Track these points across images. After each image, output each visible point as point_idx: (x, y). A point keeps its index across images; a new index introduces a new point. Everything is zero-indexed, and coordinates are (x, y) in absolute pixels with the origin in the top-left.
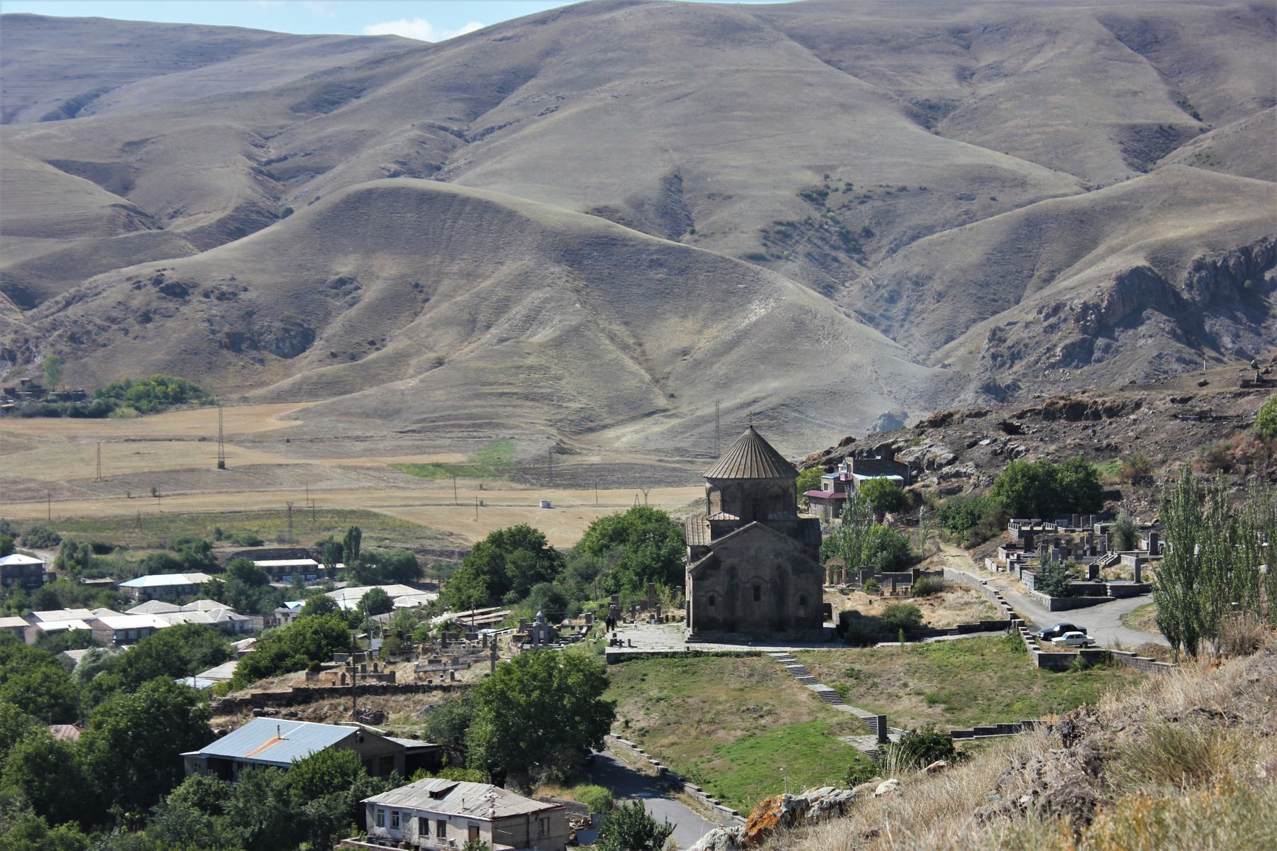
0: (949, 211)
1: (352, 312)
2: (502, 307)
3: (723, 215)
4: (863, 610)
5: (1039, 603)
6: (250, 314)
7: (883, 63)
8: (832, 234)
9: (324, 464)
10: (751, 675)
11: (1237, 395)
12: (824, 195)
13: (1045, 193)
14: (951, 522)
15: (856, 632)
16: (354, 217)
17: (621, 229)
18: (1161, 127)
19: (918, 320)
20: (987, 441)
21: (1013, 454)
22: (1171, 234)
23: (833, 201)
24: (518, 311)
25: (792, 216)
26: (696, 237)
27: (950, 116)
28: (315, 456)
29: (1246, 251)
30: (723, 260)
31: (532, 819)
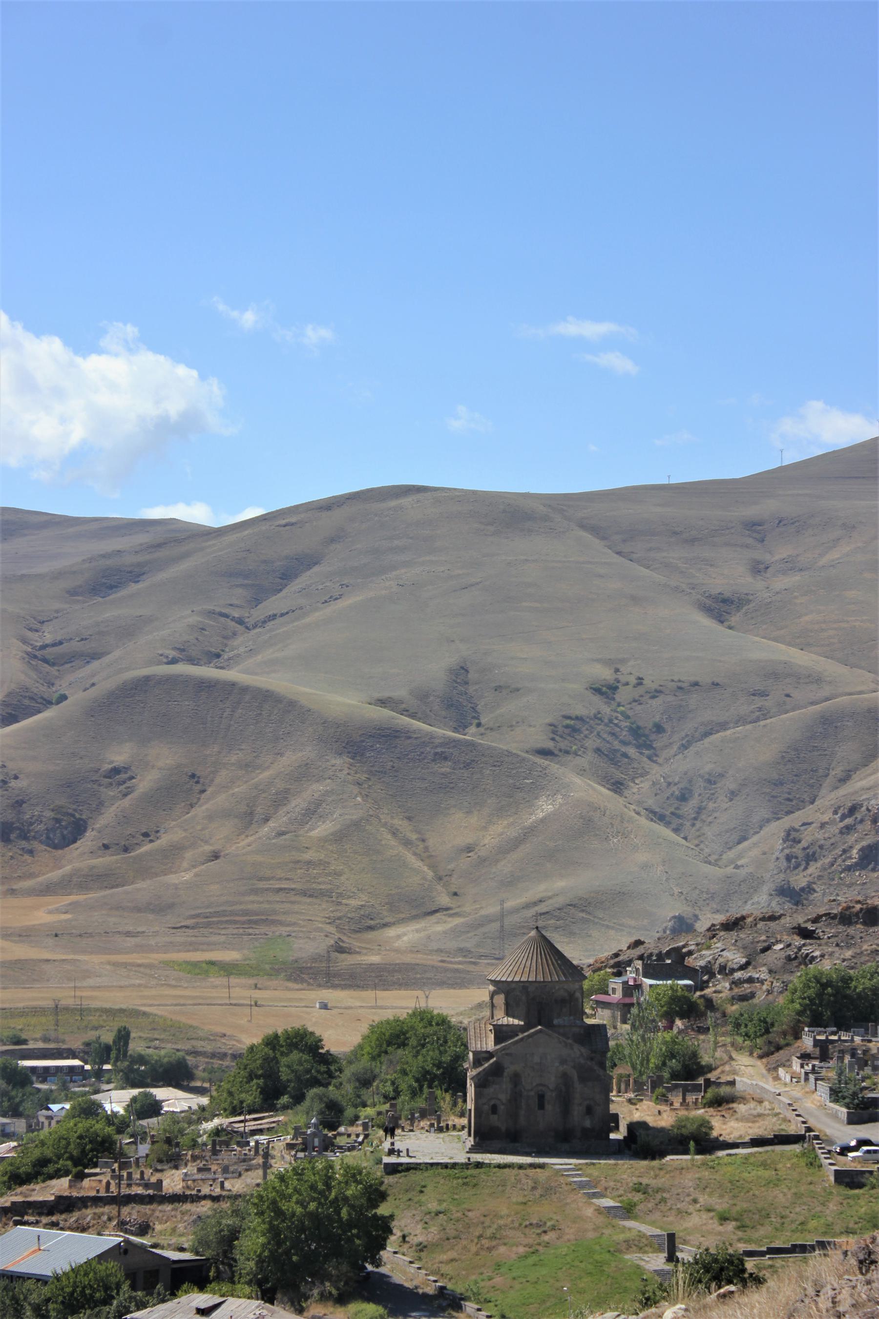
1: (126, 802)
2: (281, 799)
4: (651, 1121)
5: (835, 1116)
6: (20, 803)
8: (619, 730)
9: (94, 960)
10: (534, 1188)
12: (614, 689)
14: (743, 1030)
15: (643, 1144)
19: (710, 819)
20: (780, 946)
21: (808, 960)
24: (297, 804)
25: (579, 710)
26: (482, 730)
27: (744, 610)
28: (84, 952)
30: (509, 754)
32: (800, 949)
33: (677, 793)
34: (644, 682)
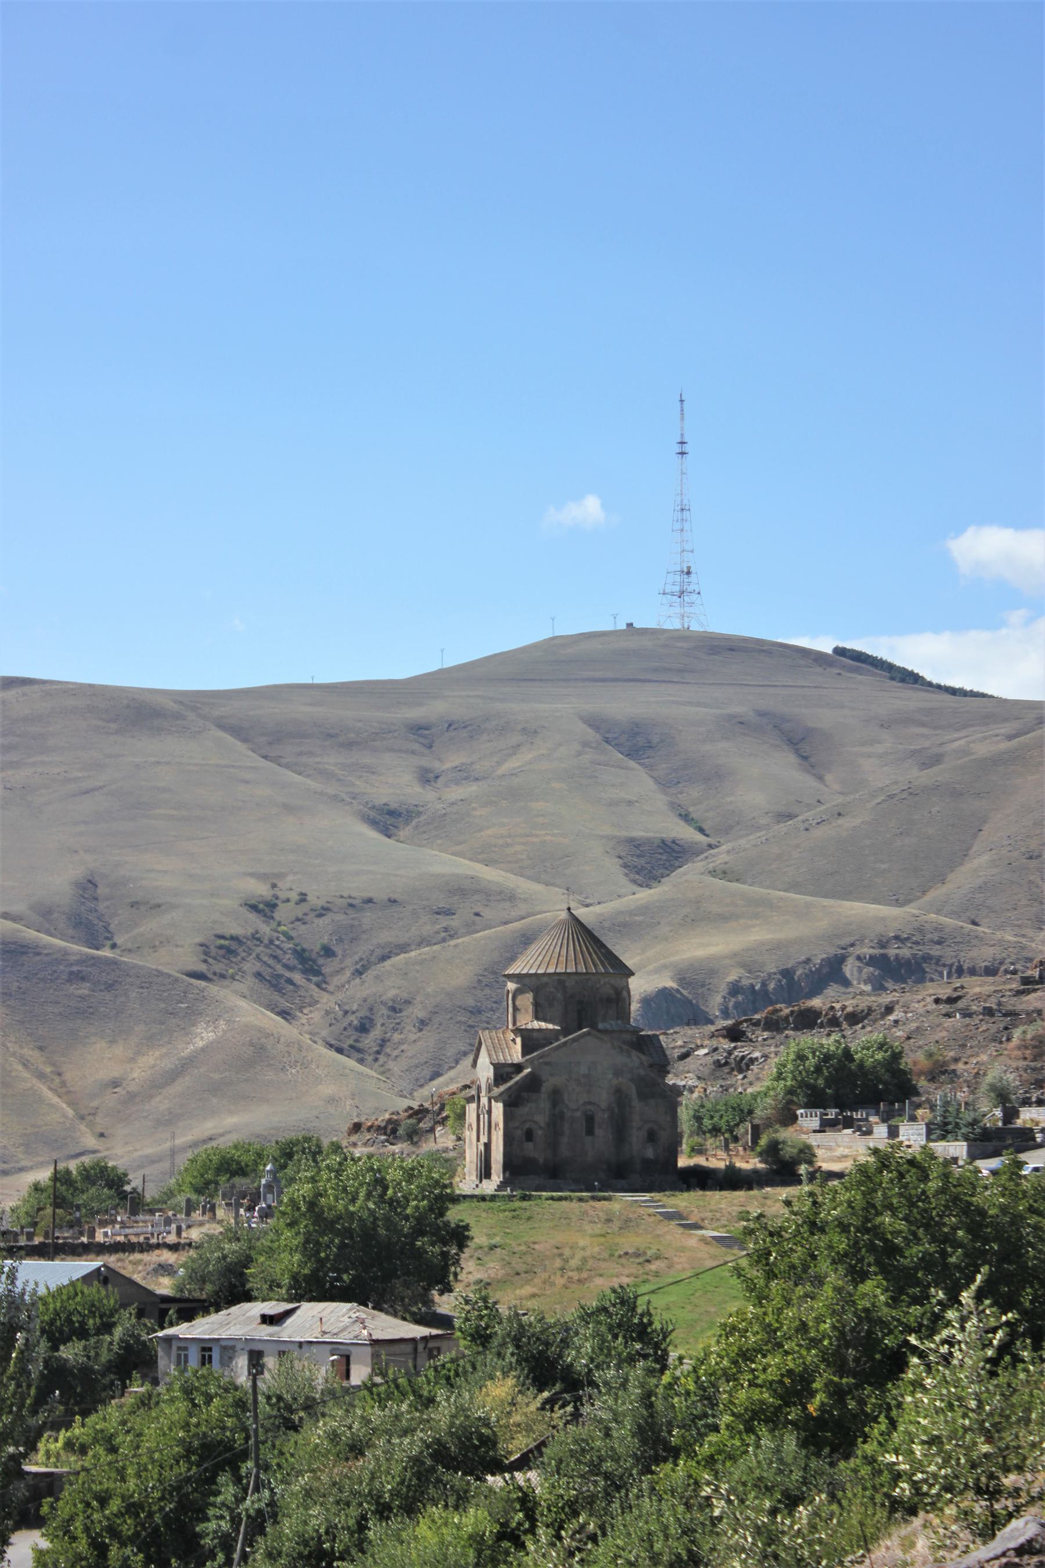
0: (427, 927)
3: (150, 926)
7: (332, 760)
8: (285, 953)
10: (609, 1220)
11: (1019, 993)
12: (273, 906)
13: (538, 908)
17: (31, 934)
18: (663, 841)
19: (395, 1053)
20: (706, 1051)
22: (700, 953)
23: (282, 913)
26: (117, 951)
27: (414, 823)
29: (787, 973)
30: (160, 974)
31: (421, 1347)
32: (730, 1053)
33: (356, 1022)
34: (308, 898)
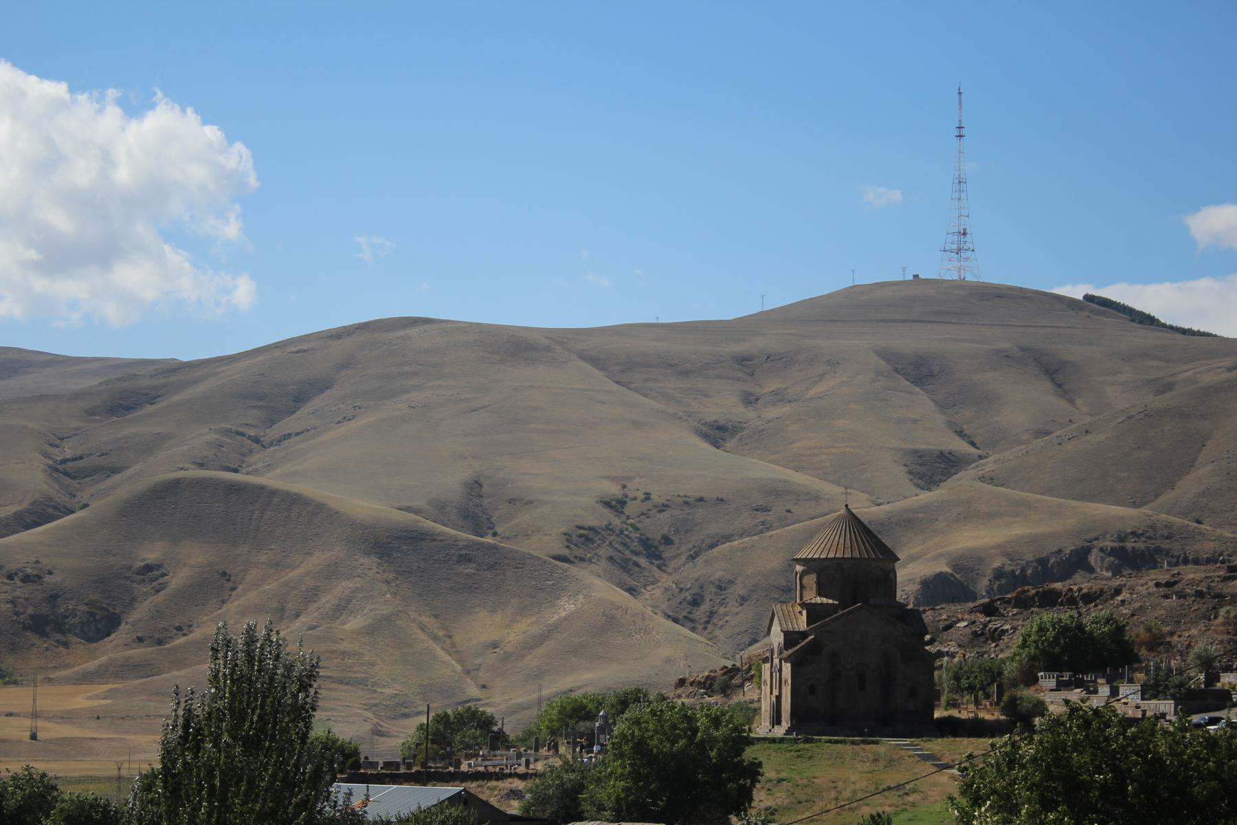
1: (160, 597)
2: (312, 595)
8: (633, 541)
12: (623, 503)
16: (163, 505)
17: (429, 524)
18: (941, 453)
19: (721, 623)
20: (965, 623)
23: (631, 508)
24: (328, 600)
25: (592, 521)
26: (498, 538)
29: (1042, 562)
30: (531, 557)
32: (985, 625)
